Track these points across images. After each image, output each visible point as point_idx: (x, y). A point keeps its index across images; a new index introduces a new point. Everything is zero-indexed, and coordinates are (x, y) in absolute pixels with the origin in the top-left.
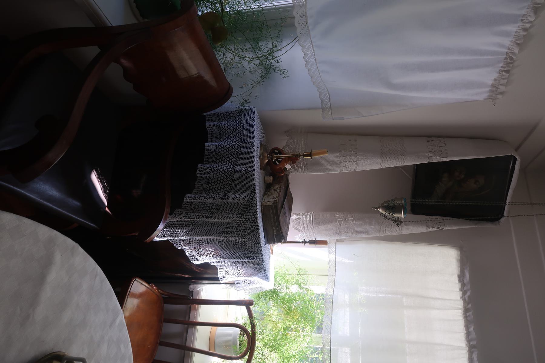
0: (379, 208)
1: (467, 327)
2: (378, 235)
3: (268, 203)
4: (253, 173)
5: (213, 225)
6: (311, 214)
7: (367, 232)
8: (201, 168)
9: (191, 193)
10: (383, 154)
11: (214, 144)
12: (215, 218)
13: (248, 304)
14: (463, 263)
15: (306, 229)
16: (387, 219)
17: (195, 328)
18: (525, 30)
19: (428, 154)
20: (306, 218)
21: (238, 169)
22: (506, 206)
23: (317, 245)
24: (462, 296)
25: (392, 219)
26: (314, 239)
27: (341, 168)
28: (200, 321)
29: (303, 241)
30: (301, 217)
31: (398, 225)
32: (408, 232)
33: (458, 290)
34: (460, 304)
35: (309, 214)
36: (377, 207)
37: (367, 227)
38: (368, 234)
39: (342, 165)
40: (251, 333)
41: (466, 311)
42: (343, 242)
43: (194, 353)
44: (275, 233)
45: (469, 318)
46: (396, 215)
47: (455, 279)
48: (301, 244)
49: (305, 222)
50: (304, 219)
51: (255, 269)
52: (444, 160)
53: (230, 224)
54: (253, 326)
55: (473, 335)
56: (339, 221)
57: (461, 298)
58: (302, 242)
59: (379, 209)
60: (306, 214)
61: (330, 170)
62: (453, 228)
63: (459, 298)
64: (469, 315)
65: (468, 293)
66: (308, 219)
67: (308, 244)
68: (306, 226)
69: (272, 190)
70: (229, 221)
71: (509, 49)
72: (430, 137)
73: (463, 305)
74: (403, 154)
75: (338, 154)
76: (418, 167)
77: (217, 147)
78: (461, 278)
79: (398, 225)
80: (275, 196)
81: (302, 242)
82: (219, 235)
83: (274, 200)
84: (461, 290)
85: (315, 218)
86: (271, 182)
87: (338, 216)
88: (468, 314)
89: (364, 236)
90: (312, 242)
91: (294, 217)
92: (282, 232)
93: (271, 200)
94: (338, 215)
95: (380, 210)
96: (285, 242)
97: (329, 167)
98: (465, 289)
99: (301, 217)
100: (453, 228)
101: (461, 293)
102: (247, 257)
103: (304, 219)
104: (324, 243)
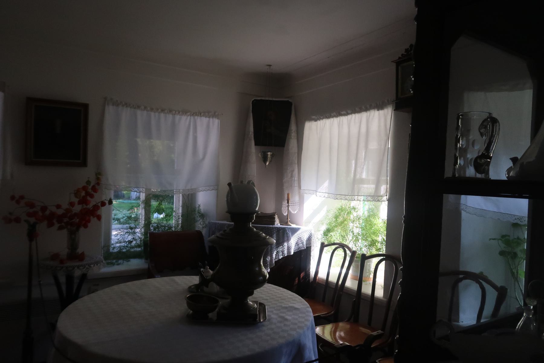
0: (266, 165)
1: (333, 117)
4: (228, 224)
7: (293, 171)
13: (323, 246)
14: (311, 119)
17: (330, 282)
18: (179, 113)
24: (314, 121)
26: (287, 201)
28: (336, 282)
29: (287, 207)
36: (265, 165)
43: (346, 285)
45: (329, 116)
46: (269, 156)
54: (334, 244)
55: (335, 113)
58: (288, 208)
59: (267, 165)
64: (328, 116)
71: (188, 116)
76: (256, 145)
81: (288, 208)
84: (320, 120)
88: (327, 117)
90: (288, 203)
95: (267, 164)
98: (319, 118)
101: (321, 120)
104: (288, 195)
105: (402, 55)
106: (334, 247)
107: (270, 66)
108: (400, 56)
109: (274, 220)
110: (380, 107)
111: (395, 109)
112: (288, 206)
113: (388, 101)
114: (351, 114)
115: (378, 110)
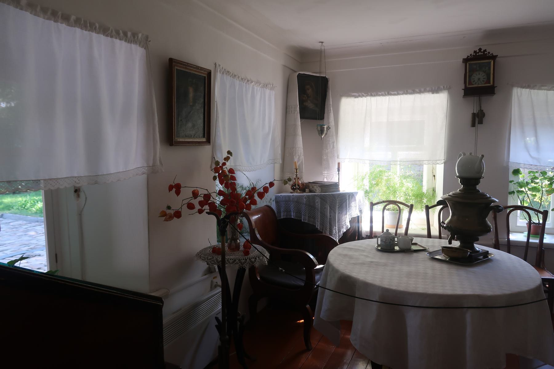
1: (379, 95)
2: (335, 137)
3: (320, 190)
4: (307, 195)
5: (330, 216)
6: (323, 172)
7: (333, 143)
8: (304, 220)
9: (316, 226)
10: (295, 135)
11: (292, 214)
12: (327, 214)
13: (372, 205)
14: (348, 95)
15: (332, 174)
16: (327, 133)
19: (296, 114)
20: (326, 174)
21: (304, 202)
22: (321, 76)
23: (340, 167)
25: (327, 131)
27: (302, 155)
30: (325, 177)
31: (330, 128)
32: (333, 122)
33: (362, 98)
34: (369, 98)
35: (324, 173)
37: (330, 142)
38: (335, 142)
39: (300, 155)
40: (387, 203)
41: (371, 95)
42: (338, 155)
43: (397, 233)
44: (334, 187)
45: (375, 94)
46: (325, 129)
47: (356, 99)
48: (340, 176)
49: (328, 174)
50: (326, 175)
51: (352, 197)
52: (298, 106)
53: (330, 208)
54: (384, 202)
55: (383, 93)
56: (327, 157)
57: (366, 97)
58: (339, 175)
60: (323, 175)
61: (302, 160)
62: (332, 111)
63: (366, 98)
65: (363, 94)
66: (326, 173)
67: (340, 172)
68: (330, 174)
69: (313, 189)
70: (328, 208)
72: (286, 112)
73: (369, 97)
74: (295, 125)
75: (295, 157)
76: (302, 117)
77: (294, 212)
78: (356, 97)
79: (330, 128)
80: (316, 187)
81: (339, 175)
82: (335, 213)
83: (318, 187)
84: (362, 97)
85: (326, 169)
86: (308, 190)
87: (325, 158)
88: (373, 95)
89: (335, 144)
90: (339, 170)
91: (325, 180)
92: (334, 184)
93: (318, 188)
94: (324, 157)
95: (323, 137)
96: (339, 183)
97: (301, 161)
98: (361, 95)
99: (325, 177)
100: (331, 100)
101: (363, 97)
102: (346, 201)
103: (326, 175)
104: (339, 164)
105: (471, 55)
106: (385, 204)
107: (322, 43)
108: (469, 55)
109: (337, 187)
110: (436, 90)
111: (463, 95)
112: (339, 174)
113: (444, 87)
114: (402, 94)
115: (433, 93)
